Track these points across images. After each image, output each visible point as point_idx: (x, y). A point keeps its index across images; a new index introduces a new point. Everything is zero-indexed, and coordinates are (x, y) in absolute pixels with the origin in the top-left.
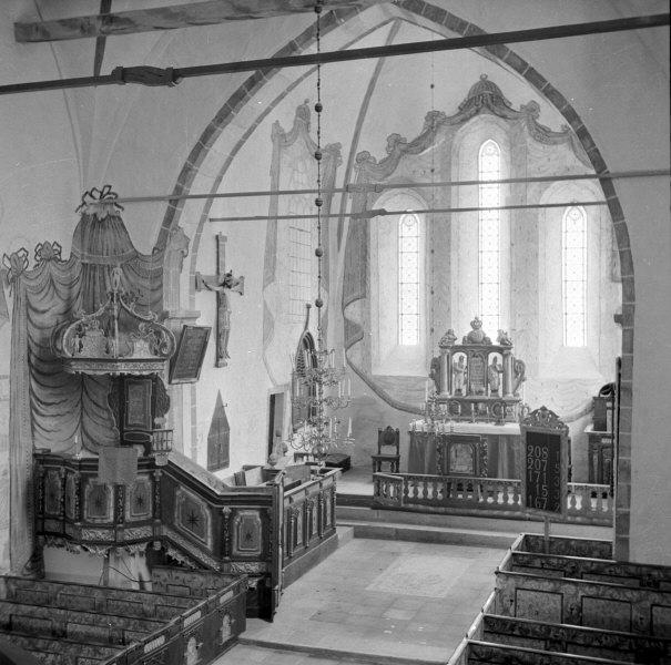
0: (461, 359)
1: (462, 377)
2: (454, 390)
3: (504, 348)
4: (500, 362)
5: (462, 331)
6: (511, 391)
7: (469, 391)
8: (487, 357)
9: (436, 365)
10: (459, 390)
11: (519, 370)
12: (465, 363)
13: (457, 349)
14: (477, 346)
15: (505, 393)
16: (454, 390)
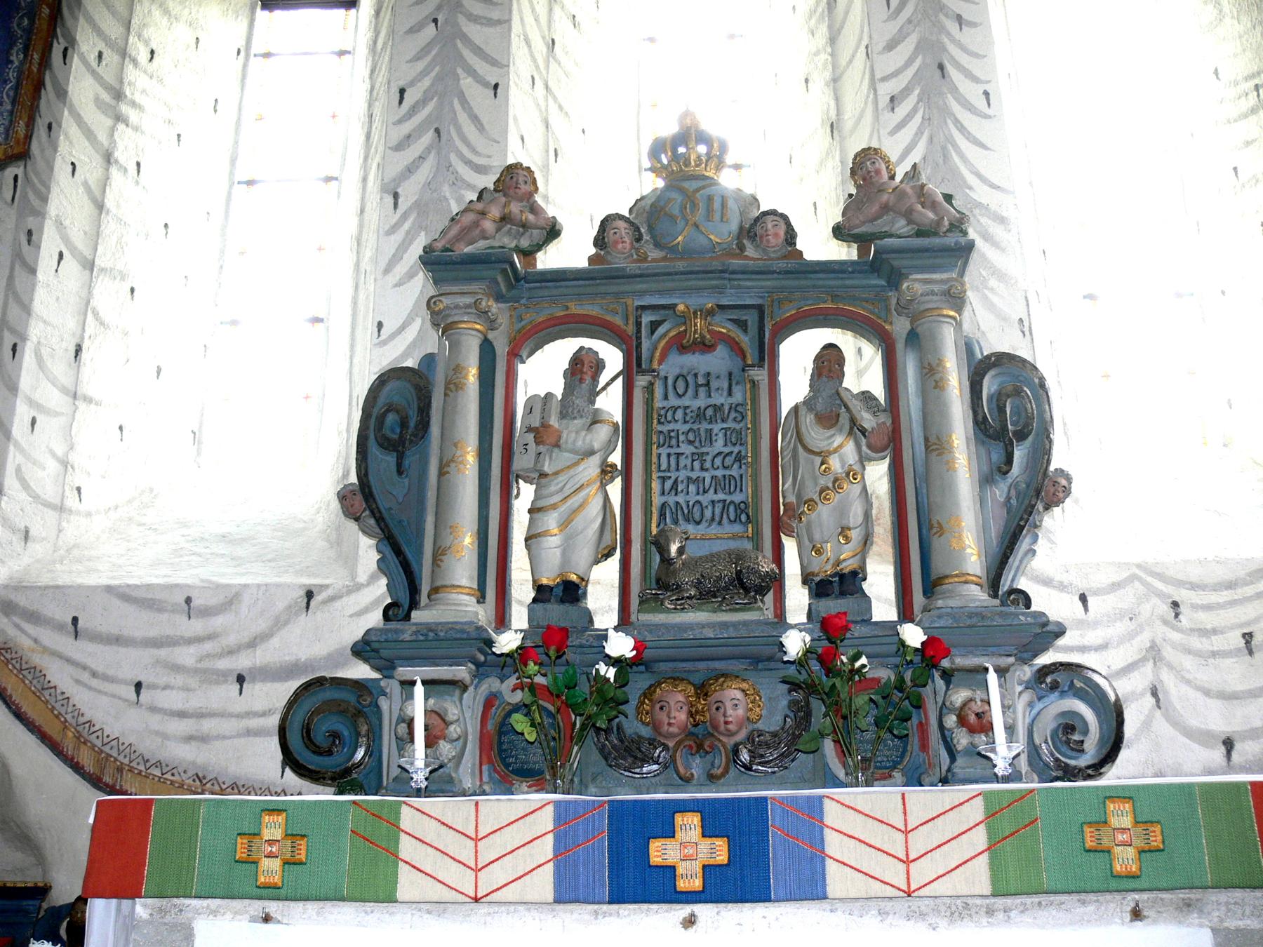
0: (582, 371)
1: (595, 498)
2: (522, 591)
3: (904, 248)
4: (864, 371)
5: (587, 194)
6: (970, 552)
7: (655, 583)
8: (767, 357)
9: (397, 422)
10: (572, 592)
11: (1012, 411)
12: (611, 402)
13: (549, 306)
14: (696, 283)
15: (921, 578)
16: (522, 591)
